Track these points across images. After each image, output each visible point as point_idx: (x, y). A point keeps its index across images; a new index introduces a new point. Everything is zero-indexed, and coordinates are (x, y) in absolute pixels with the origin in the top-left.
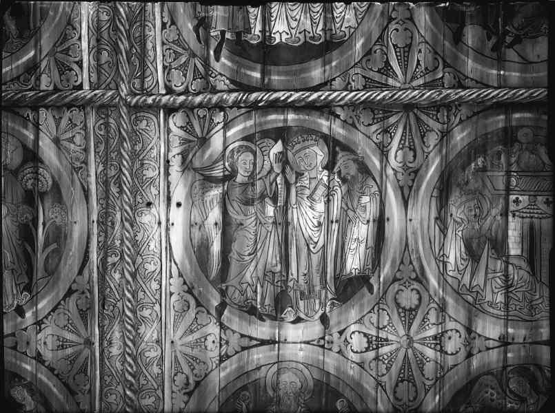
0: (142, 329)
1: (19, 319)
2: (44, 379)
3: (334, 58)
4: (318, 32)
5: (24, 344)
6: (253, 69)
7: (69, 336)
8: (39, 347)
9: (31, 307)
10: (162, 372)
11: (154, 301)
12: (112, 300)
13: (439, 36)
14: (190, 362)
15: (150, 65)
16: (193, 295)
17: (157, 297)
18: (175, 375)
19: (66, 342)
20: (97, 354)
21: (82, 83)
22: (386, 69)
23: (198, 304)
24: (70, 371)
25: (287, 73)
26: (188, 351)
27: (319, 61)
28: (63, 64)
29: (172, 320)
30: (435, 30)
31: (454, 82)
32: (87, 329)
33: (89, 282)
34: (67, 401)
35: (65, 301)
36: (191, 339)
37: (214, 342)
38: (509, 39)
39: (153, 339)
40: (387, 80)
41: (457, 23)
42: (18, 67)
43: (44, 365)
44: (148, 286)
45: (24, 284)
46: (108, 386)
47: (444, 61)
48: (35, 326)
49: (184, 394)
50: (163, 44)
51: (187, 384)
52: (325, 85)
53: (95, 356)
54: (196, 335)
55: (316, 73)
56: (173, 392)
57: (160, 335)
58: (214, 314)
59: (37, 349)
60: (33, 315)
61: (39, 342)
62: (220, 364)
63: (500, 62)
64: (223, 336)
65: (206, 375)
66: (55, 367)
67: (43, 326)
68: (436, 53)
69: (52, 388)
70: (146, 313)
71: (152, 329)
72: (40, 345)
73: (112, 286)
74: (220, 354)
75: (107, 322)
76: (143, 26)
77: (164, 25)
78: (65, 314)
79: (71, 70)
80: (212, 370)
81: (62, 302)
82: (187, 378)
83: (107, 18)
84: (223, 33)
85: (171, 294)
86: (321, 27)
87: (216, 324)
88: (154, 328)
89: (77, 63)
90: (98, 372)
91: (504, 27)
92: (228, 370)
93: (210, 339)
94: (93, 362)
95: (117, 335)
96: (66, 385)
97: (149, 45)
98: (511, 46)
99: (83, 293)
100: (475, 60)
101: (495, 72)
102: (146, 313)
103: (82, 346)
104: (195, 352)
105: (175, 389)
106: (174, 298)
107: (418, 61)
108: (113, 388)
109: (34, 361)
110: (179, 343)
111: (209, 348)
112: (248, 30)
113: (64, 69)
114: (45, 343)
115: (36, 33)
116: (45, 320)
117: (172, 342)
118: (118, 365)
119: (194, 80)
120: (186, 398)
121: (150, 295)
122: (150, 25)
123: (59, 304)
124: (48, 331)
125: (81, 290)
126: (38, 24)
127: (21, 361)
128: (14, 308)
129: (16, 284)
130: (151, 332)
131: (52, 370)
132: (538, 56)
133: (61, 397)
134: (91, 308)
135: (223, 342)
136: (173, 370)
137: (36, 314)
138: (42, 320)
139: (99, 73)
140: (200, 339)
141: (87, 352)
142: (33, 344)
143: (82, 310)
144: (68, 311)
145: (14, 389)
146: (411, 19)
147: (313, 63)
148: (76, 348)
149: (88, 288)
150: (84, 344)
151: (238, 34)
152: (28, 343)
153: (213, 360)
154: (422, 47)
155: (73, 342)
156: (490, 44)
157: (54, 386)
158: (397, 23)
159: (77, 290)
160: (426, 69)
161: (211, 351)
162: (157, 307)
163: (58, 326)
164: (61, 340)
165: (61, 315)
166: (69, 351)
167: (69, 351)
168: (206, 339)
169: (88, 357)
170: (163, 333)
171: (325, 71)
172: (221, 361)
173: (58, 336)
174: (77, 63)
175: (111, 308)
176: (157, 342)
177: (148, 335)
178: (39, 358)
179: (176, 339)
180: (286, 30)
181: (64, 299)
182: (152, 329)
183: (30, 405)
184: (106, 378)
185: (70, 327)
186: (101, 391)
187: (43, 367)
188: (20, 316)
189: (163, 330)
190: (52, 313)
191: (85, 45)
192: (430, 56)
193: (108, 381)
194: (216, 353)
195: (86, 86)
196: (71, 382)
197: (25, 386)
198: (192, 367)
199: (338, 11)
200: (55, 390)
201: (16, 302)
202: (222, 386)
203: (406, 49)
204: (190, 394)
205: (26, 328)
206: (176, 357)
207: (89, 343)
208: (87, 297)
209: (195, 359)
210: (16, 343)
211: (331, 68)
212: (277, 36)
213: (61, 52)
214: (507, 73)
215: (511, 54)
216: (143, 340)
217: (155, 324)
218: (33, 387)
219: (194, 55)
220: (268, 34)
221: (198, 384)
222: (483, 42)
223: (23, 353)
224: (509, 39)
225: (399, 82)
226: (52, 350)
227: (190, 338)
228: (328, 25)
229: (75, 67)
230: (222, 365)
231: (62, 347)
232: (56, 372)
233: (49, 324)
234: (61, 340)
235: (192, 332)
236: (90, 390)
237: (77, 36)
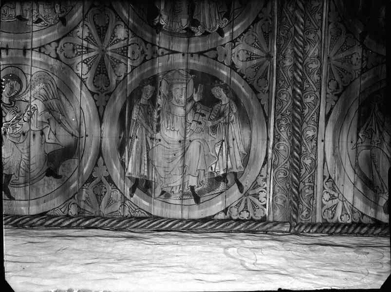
0: (308, 48)
1: (220, 38)
2: (236, 81)
5: (223, 56)
7: (256, 51)
8: (233, 58)
9: (229, 30)
10: (320, 79)
11: (317, 28)
12: (287, 26)
14: (340, 72)
16: (344, 24)
17: (319, 25)
18: (330, 81)
19: (253, 55)
20: (275, 65)
23: (348, 32)
24: (255, 76)
26: (339, 64)
29: (329, 42)
32: (268, 46)
33: (271, 13)
34: (252, 98)
35: (253, 26)
36: (342, 57)
37: (357, 59)
39: (315, 55)
43: (236, 71)
44: (313, 17)
45: (225, 13)
46: (281, 88)
48: (231, 43)
49: (335, 95)
51: (338, 87)
53: (273, 66)
54: (345, 54)
56: (327, 94)
57: (320, 52)
58: (358, 39)
59: (232, 60)
60: (230, 35)
61: (234, 55)
62: (361, 74)
64: (364, 54)
65: (351, 82)
66: (244, 73)
67: (236, 44)
69: (242, 87)
70: (311, 36)
71: (315, 48)
72: (234, 57)
73: (287, 15)
74: (362, 67)
75: (282, 42)
78: (253, 35)
80: (355, 79)
81: (251, 26)
82: (338, 84)
85: (329, 23)
87: (359, 46)
88: (316, 47)
90: (275, 78)
92: (366, 79)
93: (355, 57)
94: (272, 71)
95: (289, 51)
96: (251, 86)
99: (267, 20)
102: (311, 36)
103: (265, 59)
104: (345, 66)
105: (329, 91)
106: (331, 26)
108: (285, 89)
109: (229, 68)
110: (333, 59)
111: (354, 63)
114: (238, 56)
116: (238, 39)
117: (329, 58)
118: (290, 74)
120: (336, 98)
121: (314, 24)
123: (249, 28)
124: (240, 47)
125: (265, 18)
127: (220, 68)
128: (216, 30)
129: (218, 13)
130: (313, 50)
131: (242, 75)
133: (247, 94)
134: (272, 31)
135: (364, 59)
136: (328, 77)
137: (232, 34)
138: (236, 39)
140: (347, 56)
141: (267, 63)
142: (229, 56)
143: (265, 33)
144: (256, 33)
145: (214, 88)
148: (261, 60)
149: (271, 17)
150: (266, 57)
152: (226, 55)
153: (356, 72)
155: (257, 55)
157: (243, 87)
159: (262, 18)
161: (355, 65)
162: (319, 33)
163: (247, 43)
164: (249, 54)
165: (251, 35)
166: (255, 62)
167: (255, 62)
168: (352, 57)
169: (268, 67)
170: (322, 51)
172: (362, 72)
173: (247, 51)
175: (286, 31)
176: (318, 57)
177: (311, 53)
178: (233, 67)
179: (331, 55)
181: (253, 24)
182: (315, 48)
183: (225, 101)
184: (280, 82)
185: (256, 44)
186: (276, 91)
187: (236, 73)
188: (220, 36)
189: (323, 49)
190: (244, 34)
193: (282, 85)
194: (359, 67)
196: (255, 84)
197: (221, 86)
198: (341, 76)
200: (243, 90)
201: (218, 26)
202: (362, 90)
204: (339, 96)
205: (225, 44)
206: (331, 68)
207: (269, 56)
208: (269, 23)
209: (342, 70)
210: (217, 55)
216: (308, 56)
217: (317, 45)
218: (228, 87)
221: (345, 88)
223: (222, 63)
226: (242, 61)
227: (341, 56)
230: (363, 75)
231: (250, 59)
232: (244, 77)
233: (241, 42)
234: (249, 54)
235: (343, 51)
236: (268, 91)
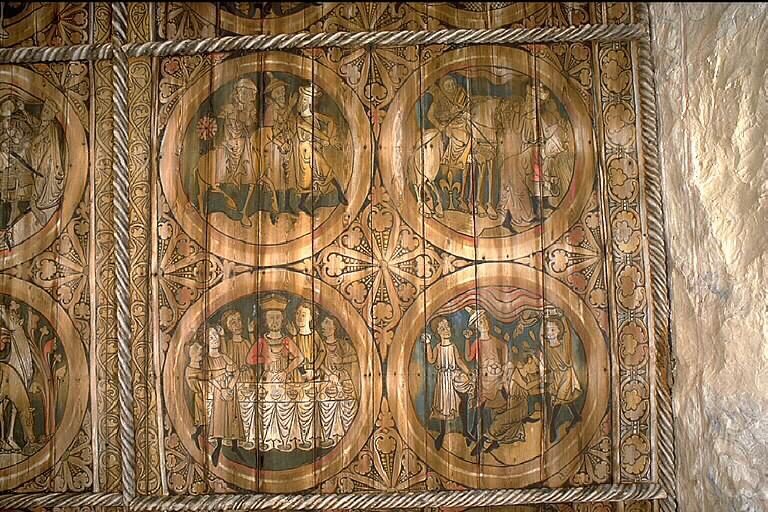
3: (324, 463)
4: (308, 439)
6: (249, 475)
13: (421, 442)
15: (153, 469)
21: (92, 485)
22: (373, 473)
25: (280, 478)
27: (310, 467)
28: (75, 467)
30: (417, 438)
31: (437, 485)
38: (486, 446)
40: (373, 483)
41: (438, 431)
42: (34, 469)
47: (428, 466)
50: (165, 449)
52: (316, 488)
55: (308, 478)
63: (479, 465)
68: (418, 458)
76: (147, 432)
77: (166, 432)
79: (83, 472)
83: (115, 425)
84: (220, 440)
86: (310, 435)
89: (88, 466)
91: (482, 433)
97: (153, 450)
98: (488, 451)
100: (457, 465)
101: (475, 474)
107: (402, 466)
112: (244, 439)
113: (76, 471)
115: (51, 440)
119: (194, 482)
122: (153, 432)
126: (53, 431)
132: (515, 460)
139: (108, 475)
146: (395, 427)
147: (303, 468)
151: (234, 442)
154: (406, 453)
156: (470, 449)
158: (381, 431)
160: (410, 473)
171: (315, 475)
174: (88, 466)
180: (279, 438)
191: (95, 448)
192: (413, 462)
195: (96, 489)
199: (326, 420)
203: (392, 455)
211: (321, 472)
212: (270, 444)
213: (73, 455)
214: (486, 476)
215: (489, 459)
219: (193, 461)
220: (261, 441)
222: (463, 446)
224: (486, 446)
225: (385, 485)
228: (317, 433)
229: (87, 469)
237: (88, 441)
